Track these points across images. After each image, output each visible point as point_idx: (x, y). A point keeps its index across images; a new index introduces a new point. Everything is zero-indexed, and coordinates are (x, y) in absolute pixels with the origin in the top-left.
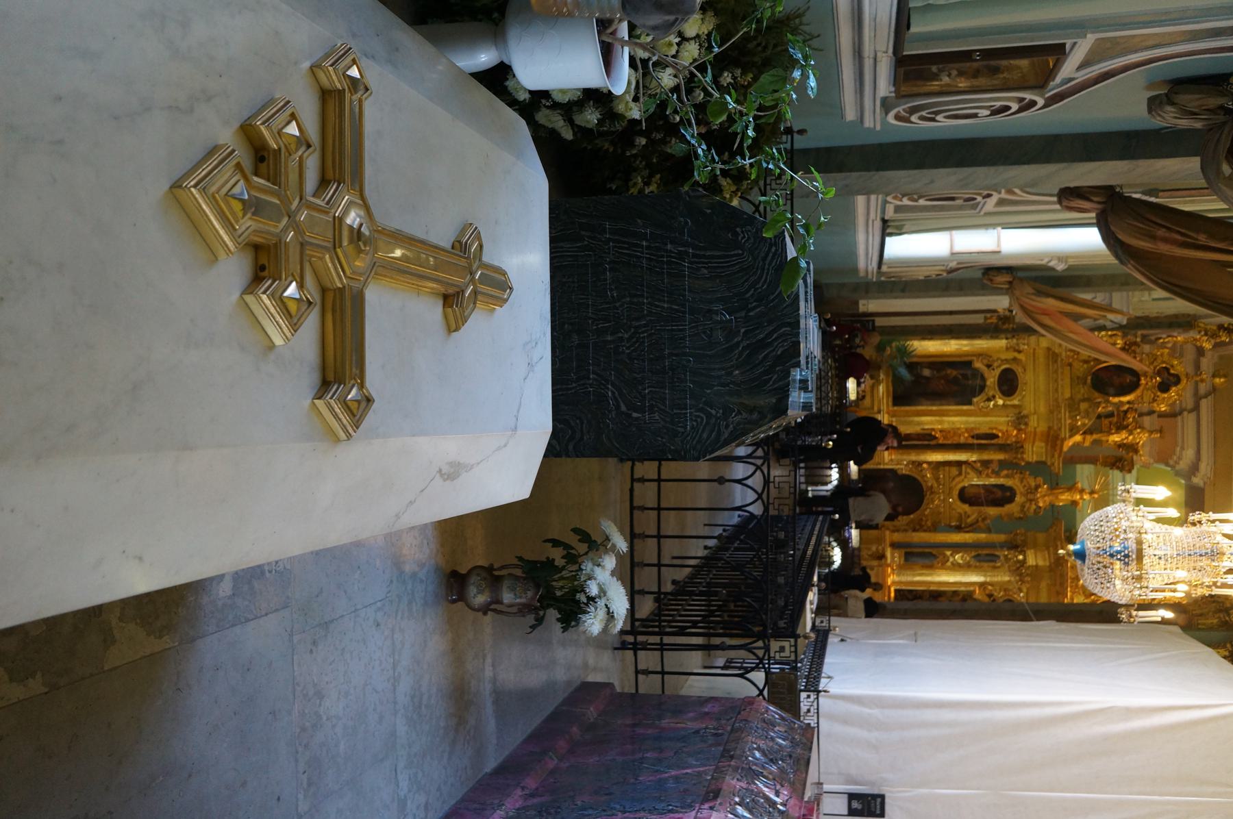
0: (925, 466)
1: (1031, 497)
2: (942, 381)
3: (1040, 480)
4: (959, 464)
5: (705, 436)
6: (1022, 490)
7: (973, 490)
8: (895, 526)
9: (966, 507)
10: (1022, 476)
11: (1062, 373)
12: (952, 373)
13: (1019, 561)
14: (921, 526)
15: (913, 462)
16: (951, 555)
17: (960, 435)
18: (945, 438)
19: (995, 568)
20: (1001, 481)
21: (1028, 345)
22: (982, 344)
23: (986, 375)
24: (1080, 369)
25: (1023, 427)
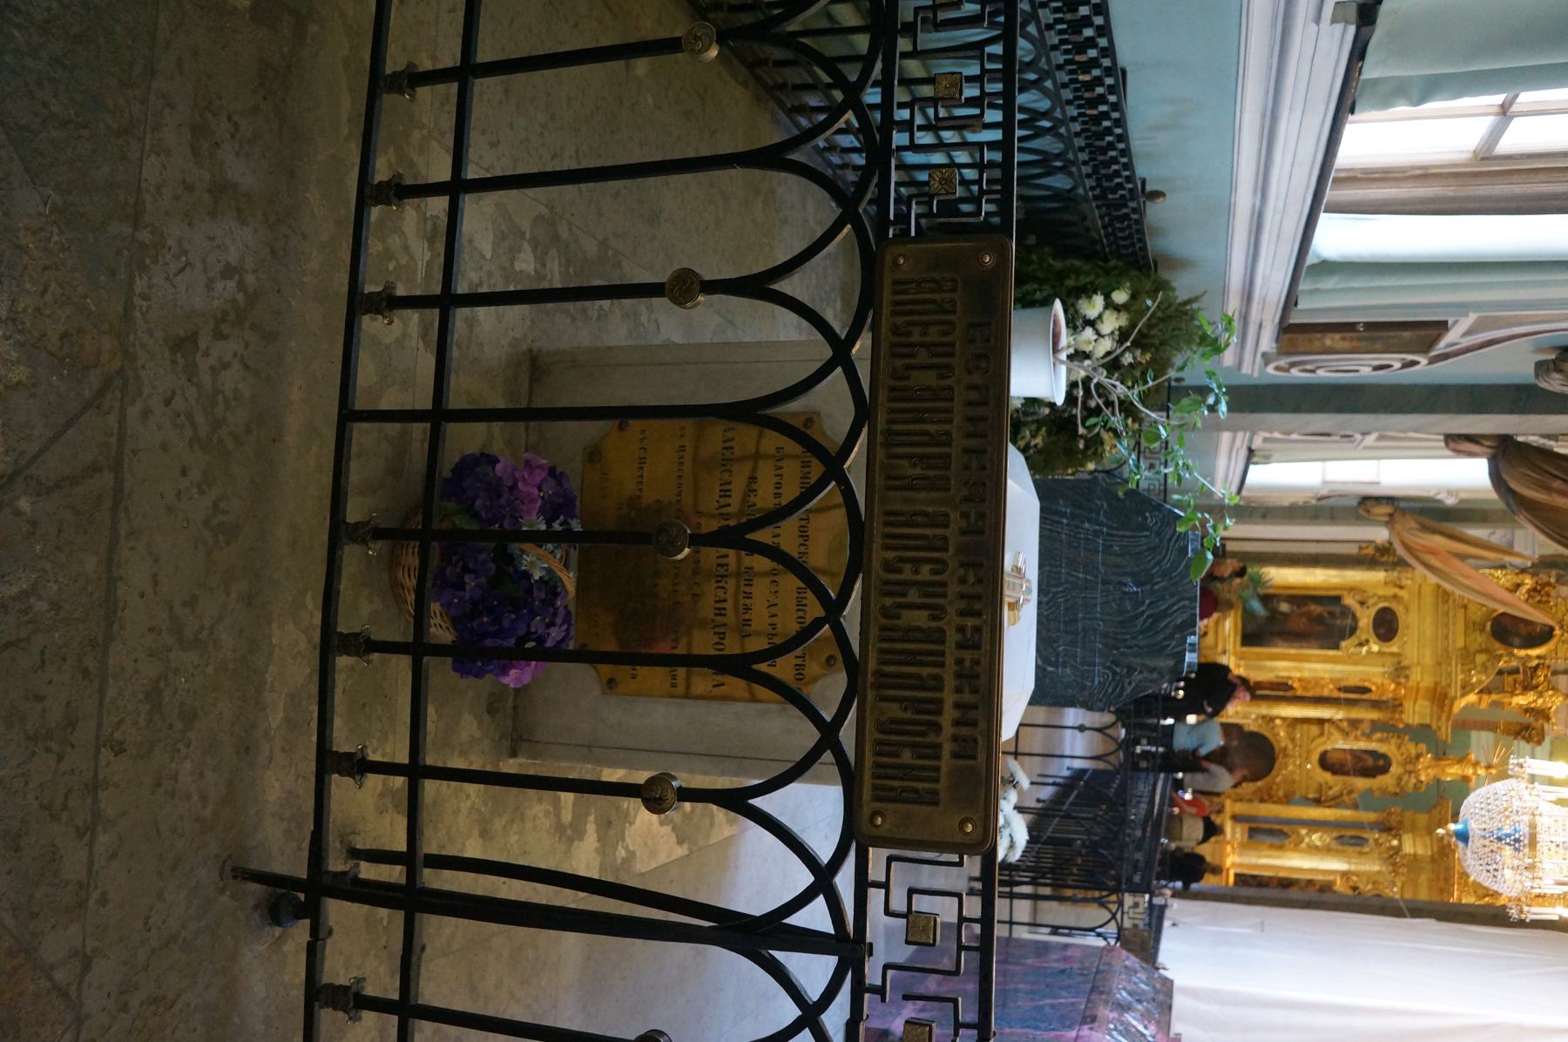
1: (1410, 767)
3: (1423, 747)
4: (1321, 722)
5: (1110, 690)
6: (1400, 758)
8: (1238, 794)
9: (1328, 776)
10: (1399, 741)
11: (1454, 616)
12: (1316, 609)
13: (1393, 848)
14: (1271, 797)
15: (1263, 717)
16: (1307, 834)
17: (1323, 687)
18: (1305, 688)
19: (1361, 854)
20: (1373, 746)
21: (1412, 579)
22: (1354, 576)
24: (1476, 614)
25: (1403, 680)
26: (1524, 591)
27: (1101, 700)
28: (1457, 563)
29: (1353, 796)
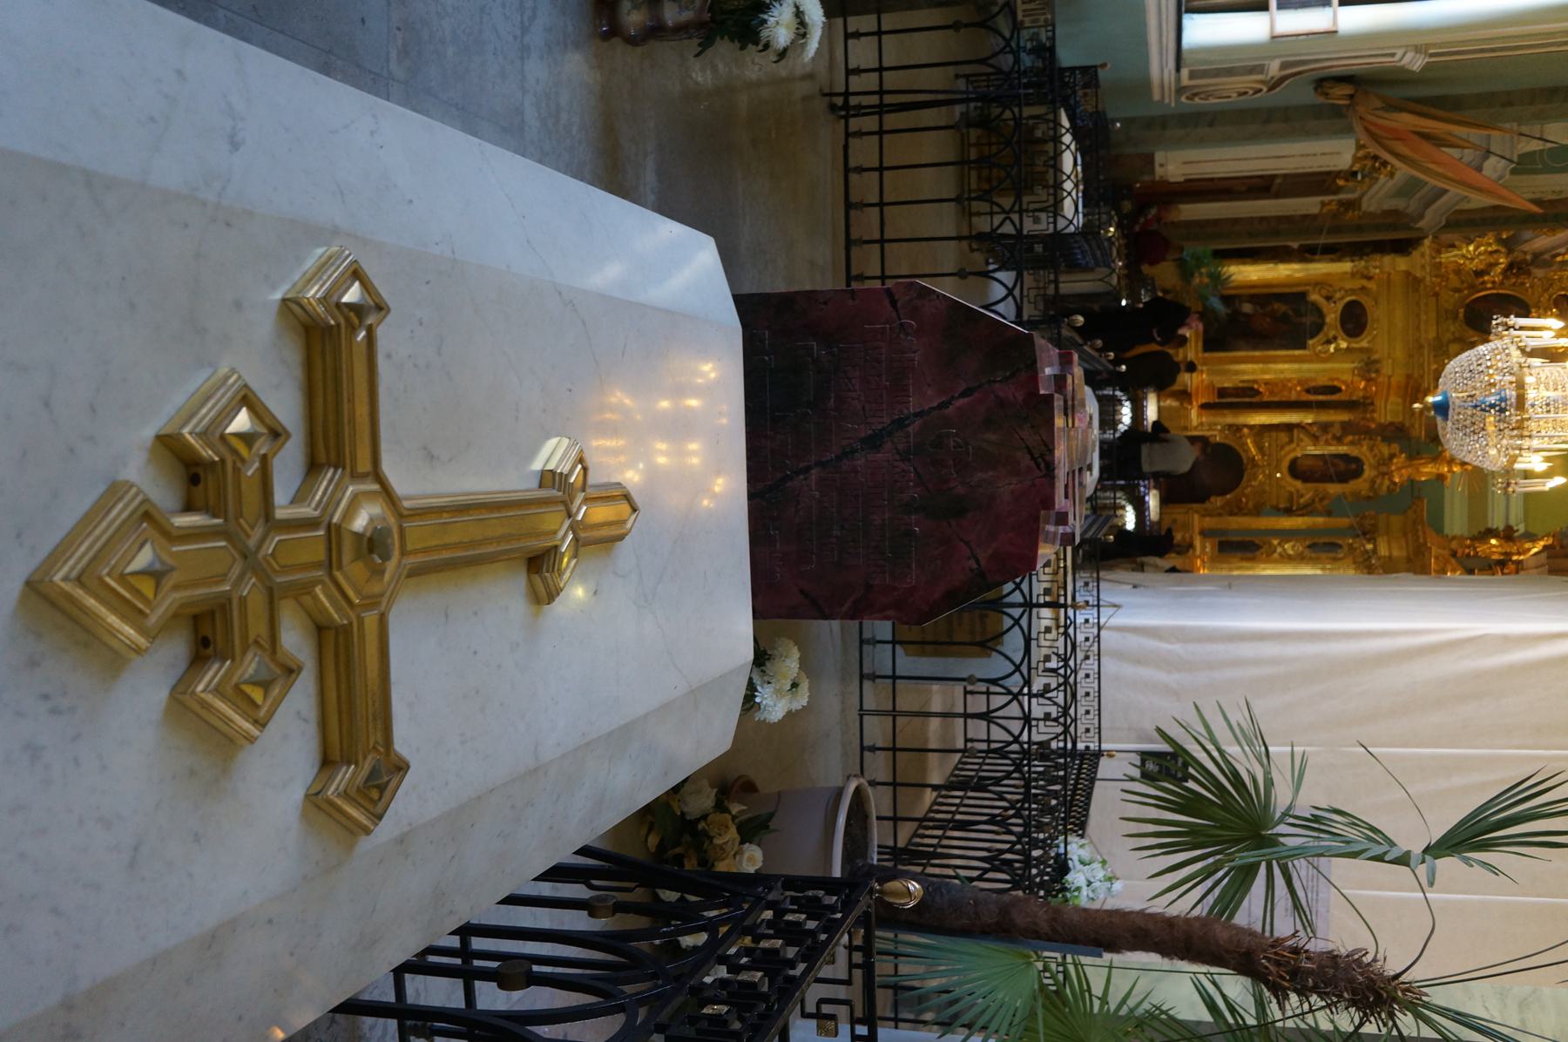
1: (1384, 469)
2: (1268, 320)
3: (1395, 447)
4: (1289, 427)
6: (1372, 461)
7: (1309, 462)
8: (1206, 510)
9: (1298, 484)
10: (1372, 442)
11: (1426, 305)
12: (1281, 308)
14: (1240, 509)
15: (1230, 426)
16: (1279, 544)
17: (1291, 389)
18: (1272, 393)
19: (1335, 560)
20: (1343, 449)
22: (1320, 268)
23: (1325, 310)
24: (1450, 299)
25: (1373, 375)
26: (1499, 270)
28: (1427, 147)
29: (1326, 502)
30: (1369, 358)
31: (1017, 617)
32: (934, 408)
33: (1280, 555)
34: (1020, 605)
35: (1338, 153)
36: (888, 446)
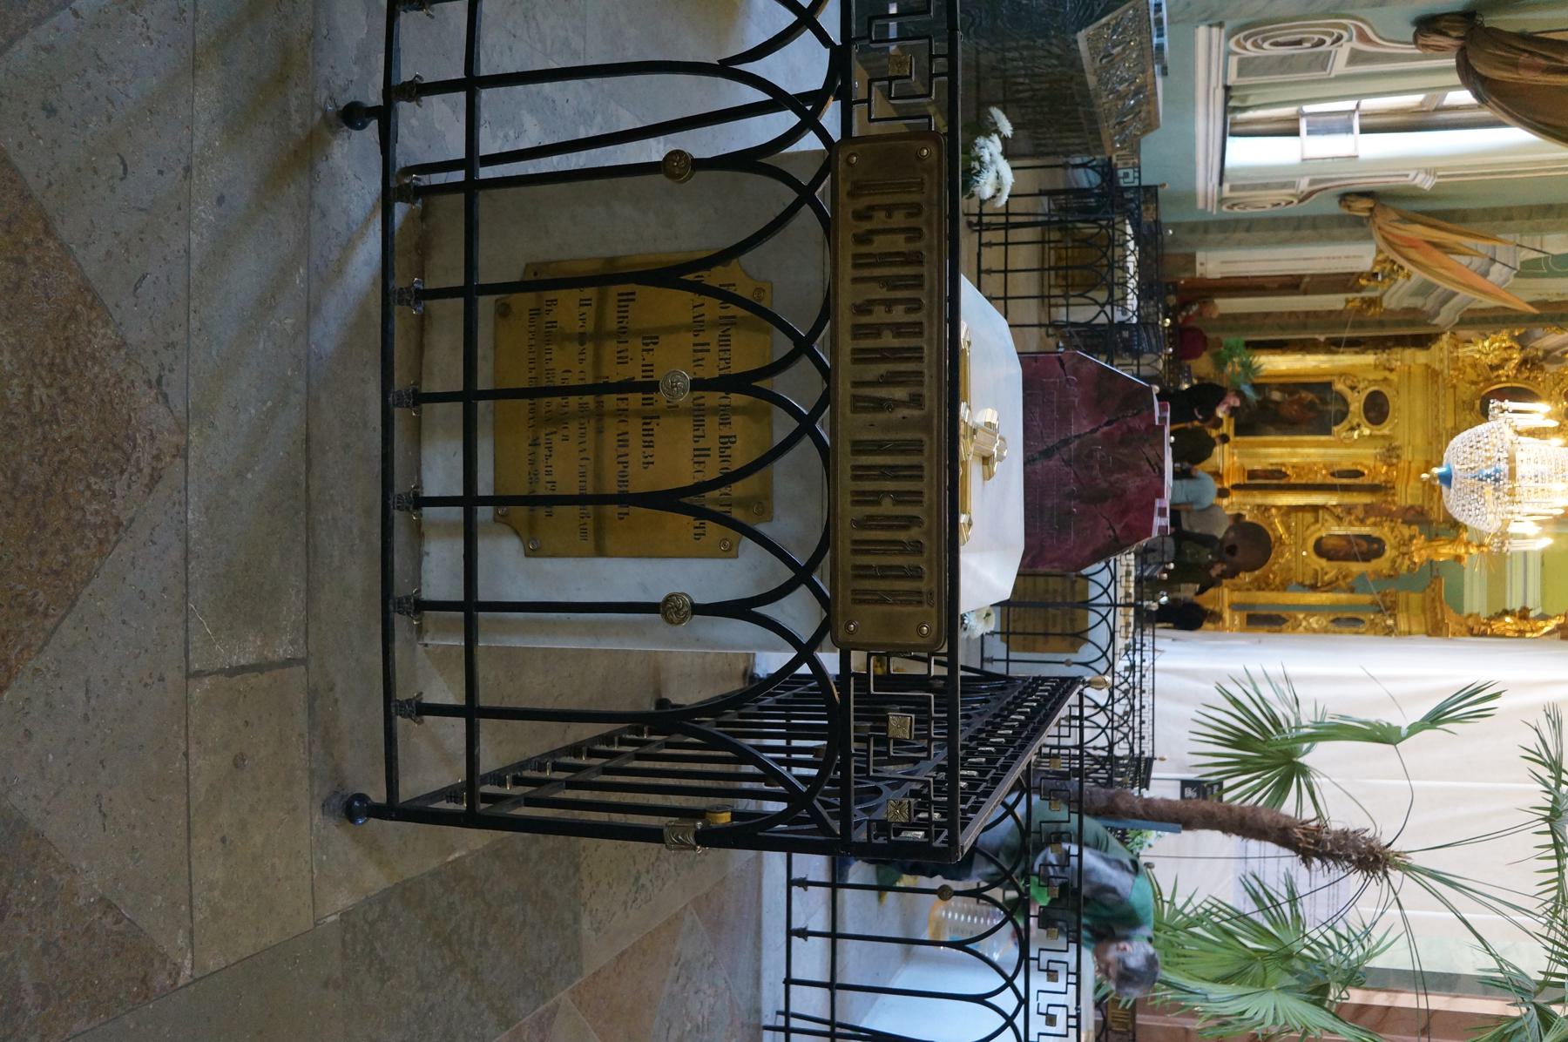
0: (1274, 511)
1: (1404, 549)
2: (1296, 407)
3: (1415, 529)
4: (1315, 509)
5: (1081, 14)
6: (1393, 541)
7: (1331, 542)
8: (1235, 585)
9: (1323, 562)
10: (1393, 524)
11: (1444, 396)
12: (1308, 396)
14: (1268, 585)
15: (1259, 506)
16: (1304, 618)
17: (1316, 472)
18: (1298, 476)
20: (1365, 530)
21: (1402, 360)
22: (1346, 360)
23: (1349, 400)
25: (1395, 461)
26: (1513, 365)
27: (1073, 24)
28: (1437, 254)
29: (1349, 580)
30: (1390, 444)
31: (1104, 614)
32: (1086, 434)
33: (1305, 628)
34: (1107, 605)
35: (1361, 257)
36: (1057, 456)
